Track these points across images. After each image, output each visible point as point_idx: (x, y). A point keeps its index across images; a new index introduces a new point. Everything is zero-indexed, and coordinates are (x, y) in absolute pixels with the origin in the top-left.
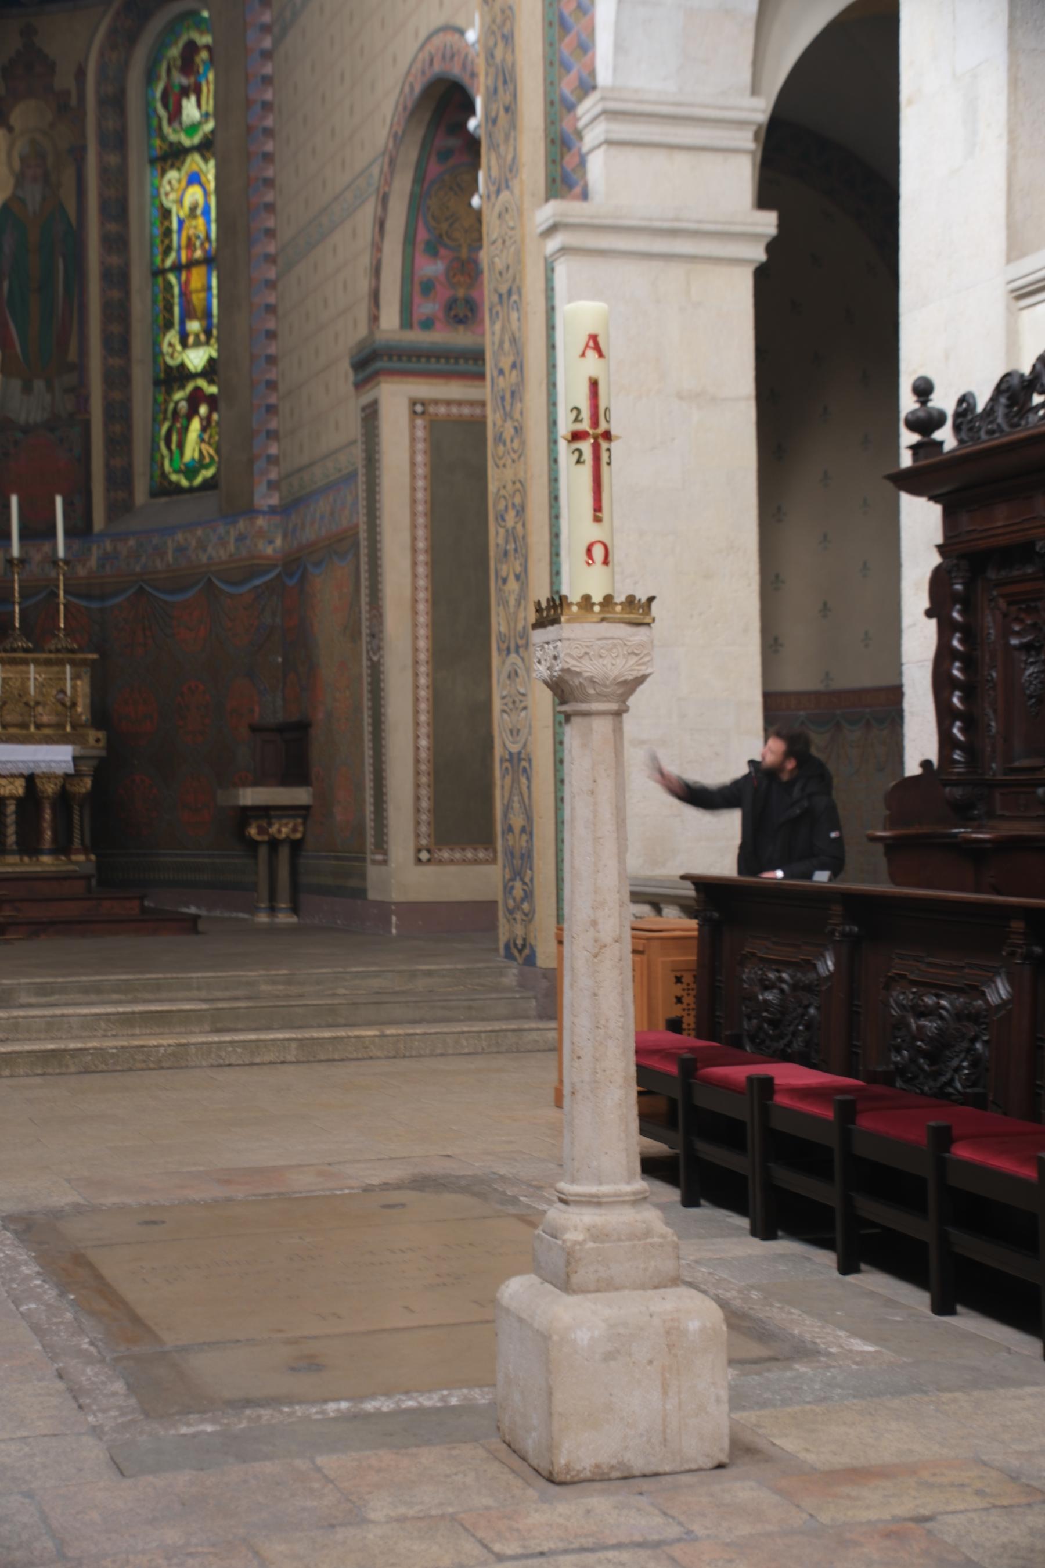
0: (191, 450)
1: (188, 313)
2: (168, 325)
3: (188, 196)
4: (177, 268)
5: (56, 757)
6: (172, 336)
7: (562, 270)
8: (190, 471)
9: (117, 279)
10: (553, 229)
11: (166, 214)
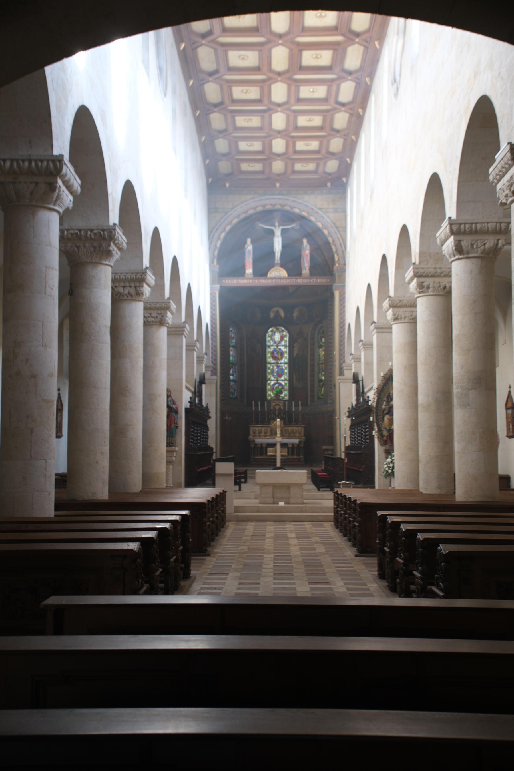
0: (322, 393)
1: (322, 371)
2: (320, 373)
3: (322, 352)
4: (321, 364)
5: (296, 441)
6: (320, 374)
7: (341, 384)
8: (322, 396)
9: (313, 365)
10: (339, 379)
11: (320, 355)
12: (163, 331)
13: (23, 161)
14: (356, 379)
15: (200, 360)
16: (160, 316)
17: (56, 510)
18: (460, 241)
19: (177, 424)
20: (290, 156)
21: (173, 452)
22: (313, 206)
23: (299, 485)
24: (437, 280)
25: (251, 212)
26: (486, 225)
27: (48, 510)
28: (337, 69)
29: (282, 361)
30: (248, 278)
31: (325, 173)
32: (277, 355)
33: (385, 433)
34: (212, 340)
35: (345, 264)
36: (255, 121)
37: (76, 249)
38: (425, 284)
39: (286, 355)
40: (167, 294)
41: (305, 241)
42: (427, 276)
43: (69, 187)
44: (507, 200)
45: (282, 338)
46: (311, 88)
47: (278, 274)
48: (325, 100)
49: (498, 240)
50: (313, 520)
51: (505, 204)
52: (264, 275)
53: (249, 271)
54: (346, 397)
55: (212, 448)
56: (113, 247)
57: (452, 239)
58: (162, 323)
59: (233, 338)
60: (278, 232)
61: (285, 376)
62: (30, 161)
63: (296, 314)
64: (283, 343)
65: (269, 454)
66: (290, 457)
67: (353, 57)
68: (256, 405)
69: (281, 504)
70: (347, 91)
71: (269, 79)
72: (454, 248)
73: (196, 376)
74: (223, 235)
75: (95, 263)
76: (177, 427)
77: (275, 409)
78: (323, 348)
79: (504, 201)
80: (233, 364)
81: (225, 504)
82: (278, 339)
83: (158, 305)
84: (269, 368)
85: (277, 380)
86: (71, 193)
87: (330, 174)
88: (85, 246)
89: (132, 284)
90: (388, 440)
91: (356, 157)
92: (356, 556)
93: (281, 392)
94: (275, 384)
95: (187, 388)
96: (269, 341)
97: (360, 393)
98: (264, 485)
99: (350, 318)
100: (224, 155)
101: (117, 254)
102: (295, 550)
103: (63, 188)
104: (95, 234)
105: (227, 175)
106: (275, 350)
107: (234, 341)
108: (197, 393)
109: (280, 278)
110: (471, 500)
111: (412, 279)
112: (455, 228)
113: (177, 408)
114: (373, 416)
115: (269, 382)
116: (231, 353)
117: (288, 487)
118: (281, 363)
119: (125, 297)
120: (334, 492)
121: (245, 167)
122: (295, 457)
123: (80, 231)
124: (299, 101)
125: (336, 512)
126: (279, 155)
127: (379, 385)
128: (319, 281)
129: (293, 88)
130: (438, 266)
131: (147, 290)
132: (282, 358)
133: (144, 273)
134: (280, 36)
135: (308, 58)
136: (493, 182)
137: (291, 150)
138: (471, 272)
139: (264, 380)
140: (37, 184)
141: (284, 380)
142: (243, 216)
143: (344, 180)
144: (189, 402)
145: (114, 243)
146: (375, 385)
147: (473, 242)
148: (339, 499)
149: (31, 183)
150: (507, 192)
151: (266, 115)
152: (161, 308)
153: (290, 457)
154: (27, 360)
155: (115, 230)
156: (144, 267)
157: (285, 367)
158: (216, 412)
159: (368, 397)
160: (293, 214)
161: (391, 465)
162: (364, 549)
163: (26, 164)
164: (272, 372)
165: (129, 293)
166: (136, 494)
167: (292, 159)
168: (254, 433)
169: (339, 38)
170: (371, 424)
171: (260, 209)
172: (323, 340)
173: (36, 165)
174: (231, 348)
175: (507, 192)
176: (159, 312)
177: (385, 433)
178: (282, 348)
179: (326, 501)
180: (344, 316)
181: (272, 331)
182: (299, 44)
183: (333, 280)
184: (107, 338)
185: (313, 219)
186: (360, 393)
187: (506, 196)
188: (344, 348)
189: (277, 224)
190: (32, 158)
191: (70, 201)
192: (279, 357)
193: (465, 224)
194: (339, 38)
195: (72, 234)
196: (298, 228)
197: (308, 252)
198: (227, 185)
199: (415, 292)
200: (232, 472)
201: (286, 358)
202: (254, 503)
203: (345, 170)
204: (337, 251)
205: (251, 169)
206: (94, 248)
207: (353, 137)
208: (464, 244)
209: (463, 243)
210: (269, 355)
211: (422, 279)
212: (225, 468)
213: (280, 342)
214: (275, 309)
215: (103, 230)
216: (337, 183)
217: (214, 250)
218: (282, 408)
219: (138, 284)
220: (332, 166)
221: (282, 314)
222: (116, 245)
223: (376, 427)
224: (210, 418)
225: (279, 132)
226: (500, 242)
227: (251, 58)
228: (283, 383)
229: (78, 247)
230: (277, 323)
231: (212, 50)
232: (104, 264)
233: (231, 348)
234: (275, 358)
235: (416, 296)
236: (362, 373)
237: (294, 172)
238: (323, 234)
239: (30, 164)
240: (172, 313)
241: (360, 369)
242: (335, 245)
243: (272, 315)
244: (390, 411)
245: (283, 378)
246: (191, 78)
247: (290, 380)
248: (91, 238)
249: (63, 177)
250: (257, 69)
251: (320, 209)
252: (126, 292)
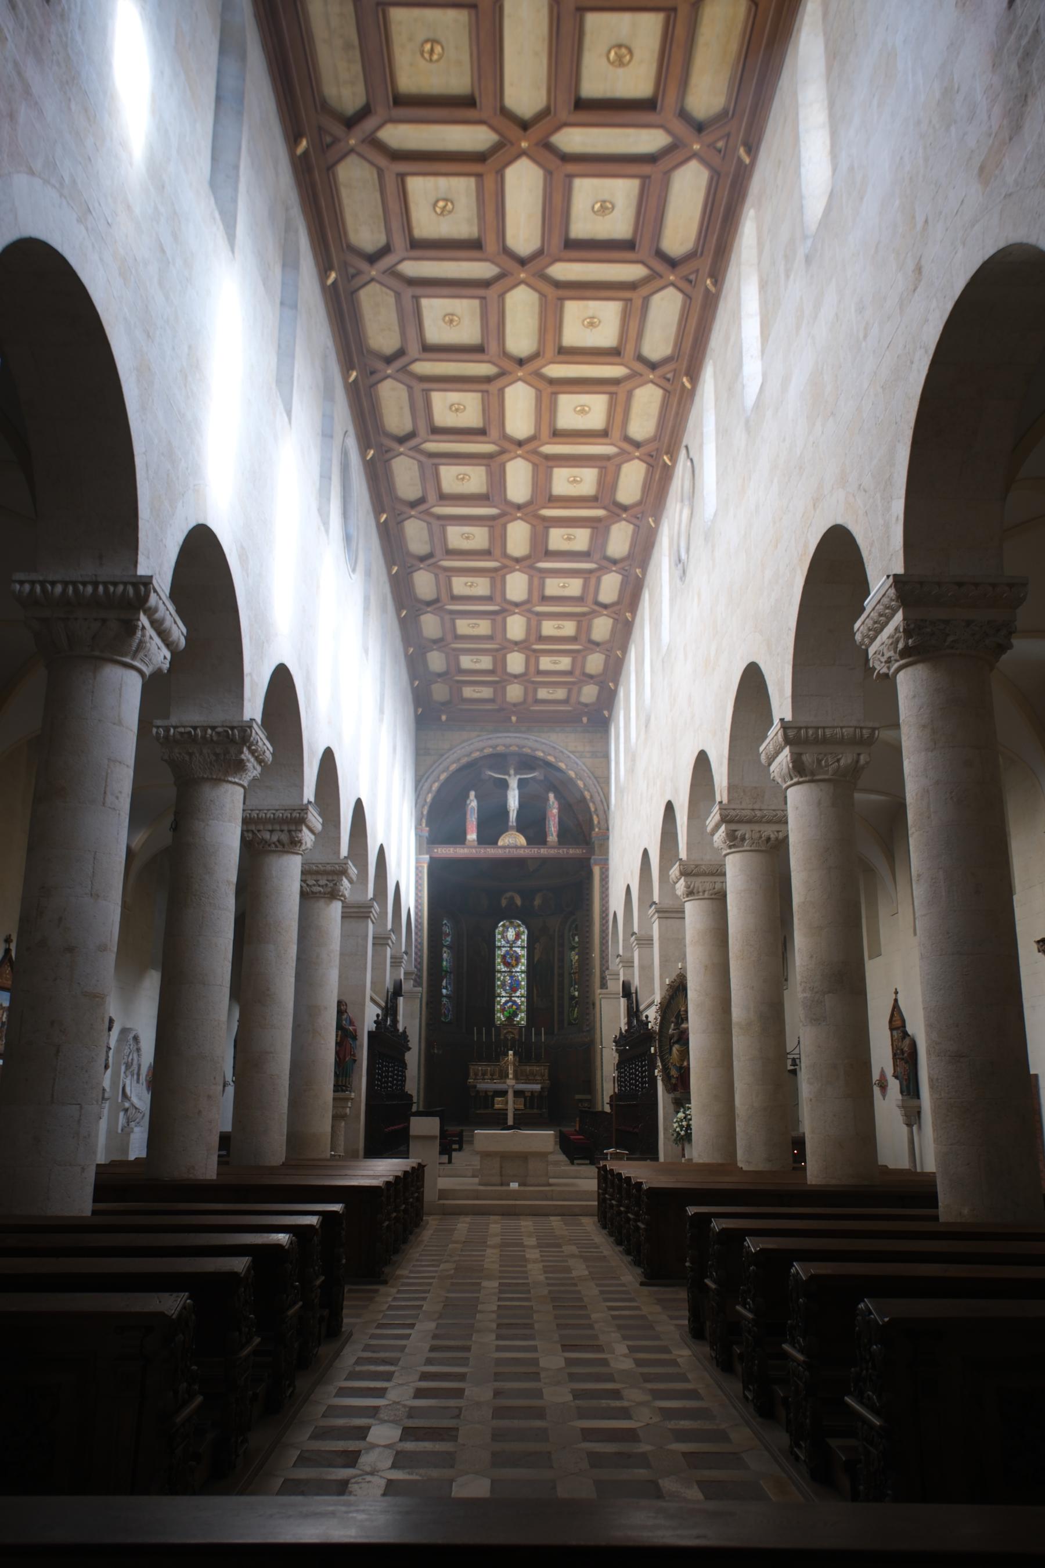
5: (537, 1087)
7: (603, 1001)
8: (575, 1020)
9: (561, 975)
12: (336, 907)
13: (84, 584)
14: (627, 991)
15: (396, 962)
16: (331, 885)
17: (95, 1200)
18: (801, 754)
19: (354, 1055)
20: (530, 678)
21: (347, 1099)
22: (562, 748)
23: (543, 1155)
24: (756, 827)
25: (477, 754)
26: (838, 730)
27: (79, 1201)
28: (597, 556)
30: (471, 846)
31: (580, 703)
32: (511, 960)
33: (674, 1072)
34: (416, 934)
35: (608, 829)
36: (483, 627)
37: (187, 758)
38: (739, 834)
39: (524, 961)
40: (344, 851)
41: (551, 796)
42: (740, 821)
43: (163, 634)
44: (889, 668)
45: (518, 936)
46: (561, 582)
47: (512, 842)
48: (580, 600)
49: (859, 755)
50: (564, 1213)
51: (886, 675)
52: (494, 842)
53: (472, 836)
54: (612, 1019)
55: (411, 1096)
56: (246, 755)
57: (787, 751)
58: (333, 894)
59: (448, 935)
60: (513, 783)
61: (522, 991)
62: (96, 585)
63: (537, 902)
64: (519, 943)
65: (497, 1106)
66: (528, 1111)
67: (619, 540)
68: (480, 1033)
69: (514, 1186)
70: (610, 586)
71: (504, 567)
72: (791, 765)
73: (389, 983)
74: (436, 786)
75: (216, 779)
76: (355, 1061)
77: (506, 1039)
78: (577, 950)
79: (884, 670)
80: (447, 972)
81: (423, 1186)
82: (511, 938)
83: (329, 868)
84: (499, 979)
85: (511, 997)
86: (168, 646)
87: (586, 705)
88: (201, 753)
89: (285, 828)
90: (680, 1085)
91: (623, 678)
92: (642, 1284)
93: (515, 1014)
94: (506, 1002)
95: (372, 1000)
96: (500, 941)
97: (633, 1012)
98: (486, 1155)
99: (616, 903)
100: (439, 675)
101: (254, 770)
102: (535, 1272)
103: (150, 632)
104: (218, 733)
105: (443, 704)
107: (449, 939)
108: (390, 1010)
109: (516, 847)
110: (833, 1182)
111: (717, 827)
112: (791, 733)
113: (355, 1030)
114: (654, 1046)
116: (445, 955)
117: (524, 1157)
119: (273, 847)
120: (599, 1168)
121: (468, 692)
122: (535, 1111)
123: (195, 728)
124: (545, 599)
125: (602, 1201)
126: (516, 676)
127: (663, 999)
128: (571, 851)
129: (536, 581)
130: (756, 806)
131: (307, 838)
132: (517, 965)
133: (304, 809)
134: (519, 507)
135: (557, 538)
136: (862, 643)
137: (532, 669)
138: (819, 803)
139: (493, 996)
140: (104, 621)
141: (520, 997)
142: (464, 760)
143: (606, 713)
144: (375, 1022)
145: (249, 748)
146: (658, 999)
147: (820, 757)
148: (607, 1178)
149: (95, 620)
150: (891, 653)
151: (499, 618)
152: (334, 873)
153: (528, 1111)
154: (60, 919)
155: (251, 727)
156: (305, 801)
157: (522, 977)
158: (420, 1042)
159: (647, 1017)
160: (536, 758)
161: (684, 1123)
162: (656, 1272)
163: (90, 589)
165: (278, 841)
166: (272, 1170)
167: (533, 682)
168: (476, 1074)
169: (600, 513)
170: (652, 1059)
171: (488, 751)
172: (577, 939)
173: (106, 590)
174: (445, 949)
175: (888, 654)
176: (330, 878)
177: (674, 1072)
178: (518, 950)
179: (585, 1181)
180: (607, 902)
181: (503, 925)
182: (544, 519)
183: (591, 851)
184: (230, 902)
185: (562, 765)
186: (633, 1012)
187: (889, 661)
188: (607, 948)
189: (512, 772)
190: (100, 579)
191: (165, 658)
192: (514, 962)
193: (807, 728)
194: (600, 513)
195: (181, 733)
196: (542, 778)
197: (555, 811)
198: (444, 718)
199: (723, 846)
200: (437, 1132)
201: (523, 964)
202: (470, 1183)
203: (608, 698)
204: (596, 810)
205: (476, 695)
206: (217, 755)
207: (619, 653)
208: (807, 758)
209: (804, 758)
211: (733, 827)
212: (424, 1126)
213: (514, 942)
214: (509, 894)
215: (232, 728)
216: (597, 719)
217: (423, 807)
218: (517, 1037)
219: (294, 828)
220: (589, 693)
221: (519, 901)
222: (253, 752)
223: (659, 1064)
224: (409, 1049)
225: (516, 643)
226: (862, 757)
227: (478, 537)
228: (518, 1001)
229: (191, 755)
230: (511, 914)
231: (424, 525)
232: (231, 782)
233: (445, 949)
234: (507, 964)
235: (724, 852)
236: (636, 982)
237: (537, 701)
238: (577, 785)
239: (96, 588)
240: (351, 881)
241: (633, 978)
242: (594, 803)
243: (504, 903)
244: (683, 1038)
245: (518, 994)
246: (395, 564)
247: (529, 996)
248: (212, 740)
249: (150, 613)
250: (486, 554)
251: (572, 752)
252: (275, 838)
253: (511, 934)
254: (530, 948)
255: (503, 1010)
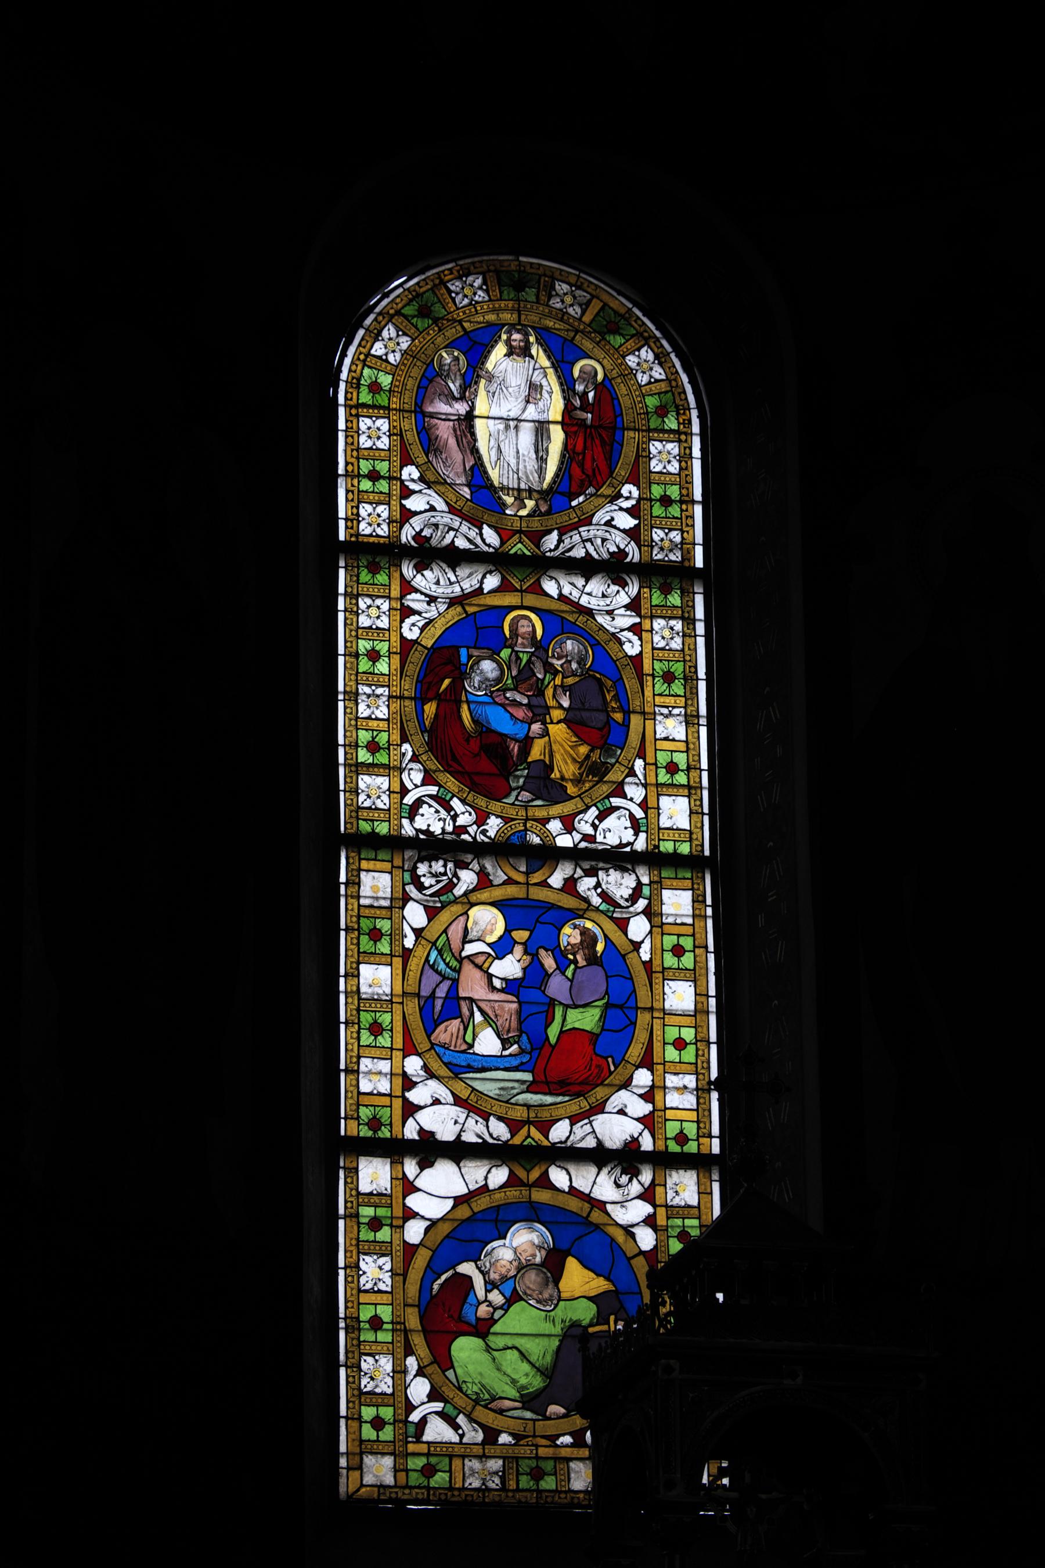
29: (616, 831)
45: (597, 444)
64: (611, 526)
84: (376, 931)
94: (474, 1225)
106: (481, 624)
115: (374, 1174)
118: (596, 858)
132: (600, 776)
164: (438, 1007)
210: (369, 706)
234: (475, 760)
253: (514, 413)
254: (738, 585)
255: (442, 1315)
